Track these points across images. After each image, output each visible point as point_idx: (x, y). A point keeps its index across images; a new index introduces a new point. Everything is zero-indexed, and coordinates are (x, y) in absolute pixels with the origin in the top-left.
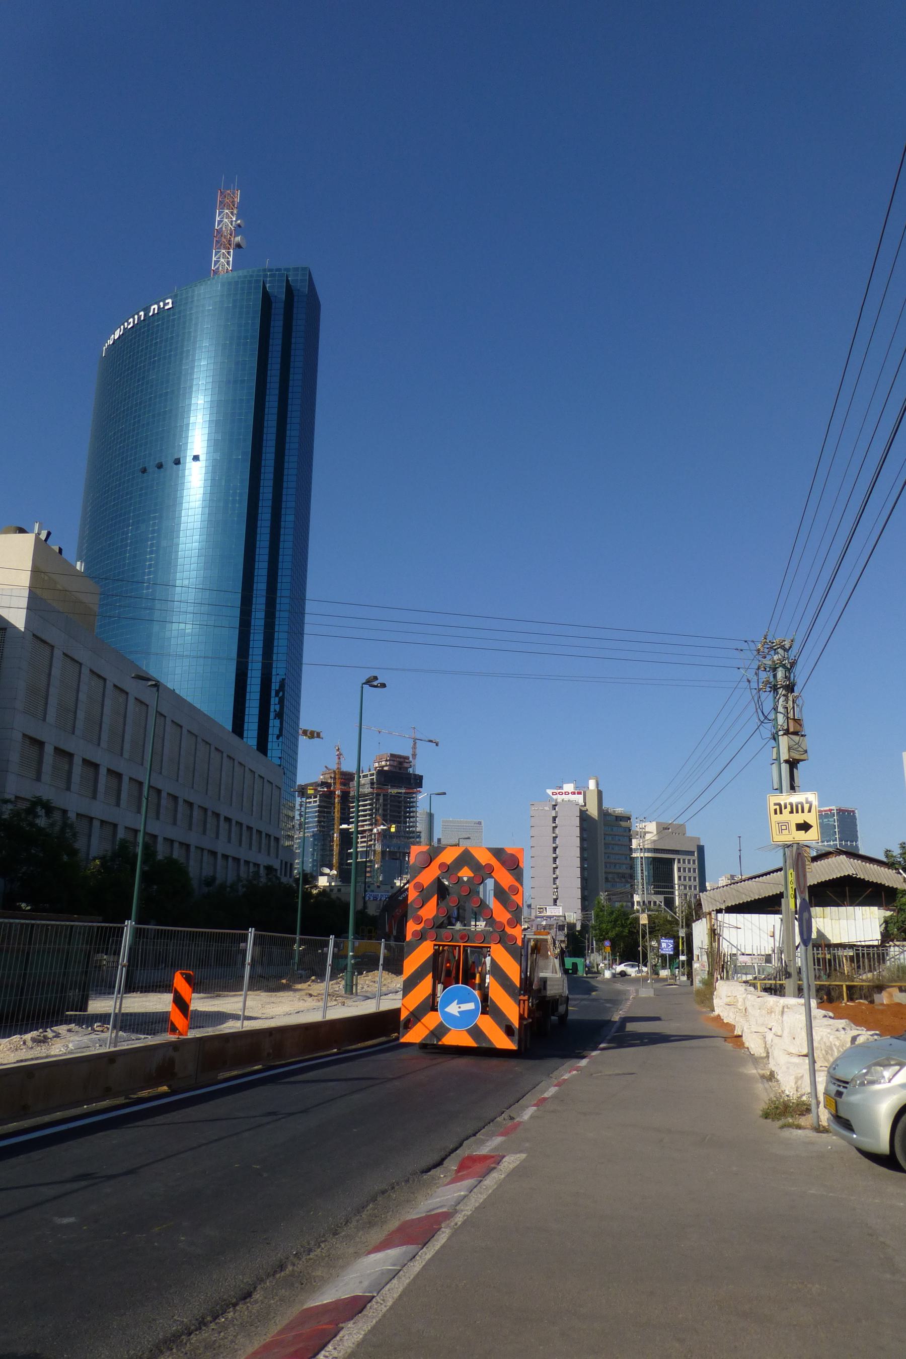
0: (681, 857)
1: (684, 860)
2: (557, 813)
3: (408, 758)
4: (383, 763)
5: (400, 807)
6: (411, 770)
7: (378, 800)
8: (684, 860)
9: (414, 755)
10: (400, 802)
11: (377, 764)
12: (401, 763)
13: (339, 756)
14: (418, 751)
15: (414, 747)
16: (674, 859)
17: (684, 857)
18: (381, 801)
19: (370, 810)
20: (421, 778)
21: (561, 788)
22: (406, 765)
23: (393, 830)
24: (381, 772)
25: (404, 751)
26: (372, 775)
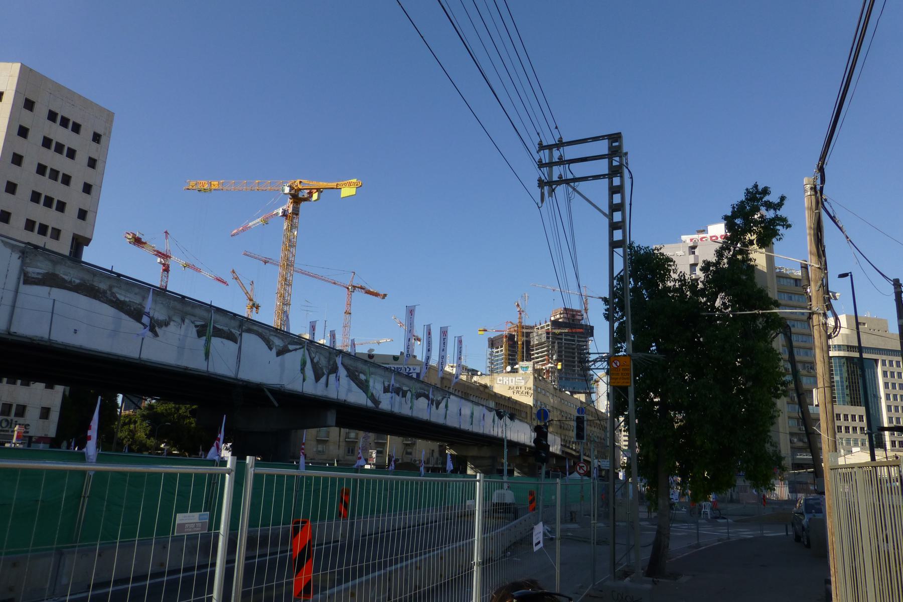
0: (887, 358)
1: (891, 362)
2: (697, 258)
3: (580, 311)
4: (558, 316)
5: (574, 353)
6: (583, 322)
7: (553, 347)
8: (891, 362)
9: (586, 310)
10: (574, 349)
11: (553, 319)
12: (573, 316)
13: (520, 313)
14: (589, 307)
15: (586, 303)
16: (876, 361)
17: (891, 358)
18: (556, 347)
19: (548, 355)
20: (592, 328)
21: (704, 231)
22: (579, 318)
23: (559, 367)
24: (555, 323)
25: (576, 306)
26: (548, 325)
